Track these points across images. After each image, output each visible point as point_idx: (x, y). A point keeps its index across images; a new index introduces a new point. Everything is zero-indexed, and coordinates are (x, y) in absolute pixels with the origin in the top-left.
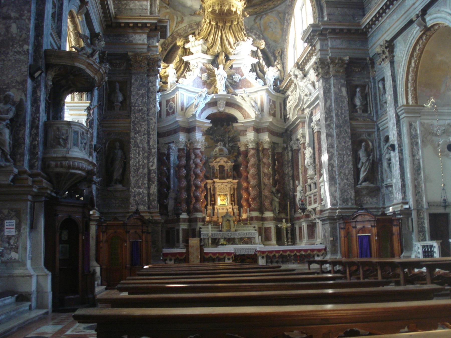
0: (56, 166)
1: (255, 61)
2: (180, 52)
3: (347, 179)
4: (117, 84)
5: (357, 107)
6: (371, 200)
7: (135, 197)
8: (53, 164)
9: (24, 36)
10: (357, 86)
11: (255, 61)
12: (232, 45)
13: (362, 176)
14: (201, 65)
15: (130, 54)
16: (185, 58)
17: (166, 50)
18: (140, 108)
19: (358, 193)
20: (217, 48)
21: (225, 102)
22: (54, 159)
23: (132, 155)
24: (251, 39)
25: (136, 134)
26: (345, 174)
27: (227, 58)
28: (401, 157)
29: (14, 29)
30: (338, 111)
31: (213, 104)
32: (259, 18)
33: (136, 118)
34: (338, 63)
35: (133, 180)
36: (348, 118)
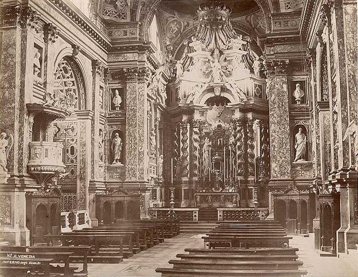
0: (34, 169)
1: (245, 53)
2: (186, 51)
3: (285, 157)
4: (117, 92)
5: (296, 99)
6: (305, 173)
7: (129, 171)
8: (33, 169)
9: (12, 98)
10: (297, 82)
11: (245, 53)
12: (225, 43)
13: (298, 154)
14: (201, 60)
15: (125, 70)
16: (190, 55)
17: (176, 48)
18: (133, 108)
19: (293, 167)
20: (212, 46)
21: (220, 89)
22: (33, 166)
23: (127, 142)
24: (241, 36)
25: (129, 126)
26: (283, 153)
27: (221, 53)
28: (318, 142)
29: (7, 94)
30: (279, 103)
31: (211, 90)
32: (249, 17)
33: (130, 115)
34: (281, 65)
35: (127, 161)
36: (287, 108)
